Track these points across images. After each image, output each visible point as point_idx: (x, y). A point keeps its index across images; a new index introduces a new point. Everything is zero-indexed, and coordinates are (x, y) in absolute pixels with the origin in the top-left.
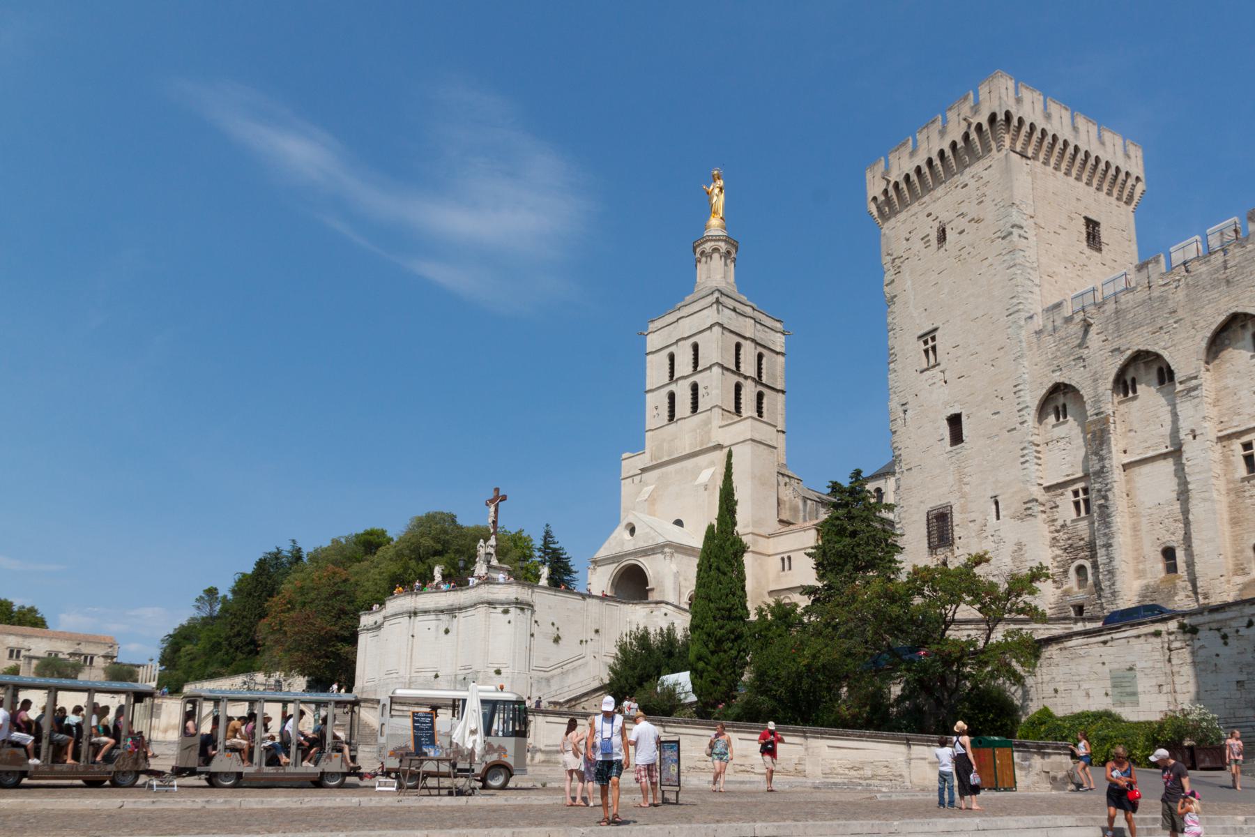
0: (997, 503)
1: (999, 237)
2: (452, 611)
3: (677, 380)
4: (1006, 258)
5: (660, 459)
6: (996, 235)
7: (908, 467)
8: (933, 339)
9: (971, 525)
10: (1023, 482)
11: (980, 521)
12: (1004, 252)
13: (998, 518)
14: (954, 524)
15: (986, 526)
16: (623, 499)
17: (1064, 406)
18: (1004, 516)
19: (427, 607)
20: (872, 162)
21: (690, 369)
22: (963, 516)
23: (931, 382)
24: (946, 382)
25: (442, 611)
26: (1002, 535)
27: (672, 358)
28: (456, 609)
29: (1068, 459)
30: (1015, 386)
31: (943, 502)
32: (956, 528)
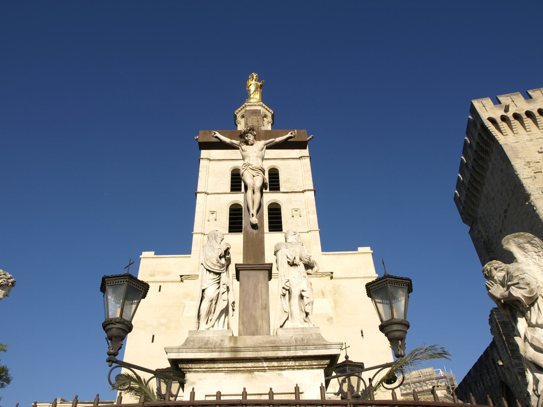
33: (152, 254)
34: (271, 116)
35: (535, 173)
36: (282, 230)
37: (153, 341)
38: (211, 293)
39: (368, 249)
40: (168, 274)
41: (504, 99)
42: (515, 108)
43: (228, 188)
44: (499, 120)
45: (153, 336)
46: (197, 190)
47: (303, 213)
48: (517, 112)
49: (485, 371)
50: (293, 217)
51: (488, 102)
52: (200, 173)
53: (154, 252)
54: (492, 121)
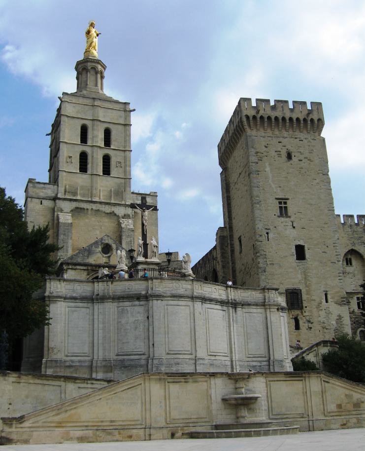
0: (326, 295)
2: (235, 305)
4: (326, 184)
6: (321, 172)
8: (285, 203)
10: (340, 288)
12: (325, 181)
13: (327, 302)
14: (303, 299)
15: (321, 304)
17: (350, 259)
18: (331, 302)
22: (308, 296)
23: (285, 224)
24: (294, 227)
26: (331, 310)
27: (84, 131)
29: (354, 283)
31: (296, 287)
38: (141, 251)
42: (263, 112)
44: (251, 118)
47: (123, 165)
48: (264, 115)
49: (207, 262)
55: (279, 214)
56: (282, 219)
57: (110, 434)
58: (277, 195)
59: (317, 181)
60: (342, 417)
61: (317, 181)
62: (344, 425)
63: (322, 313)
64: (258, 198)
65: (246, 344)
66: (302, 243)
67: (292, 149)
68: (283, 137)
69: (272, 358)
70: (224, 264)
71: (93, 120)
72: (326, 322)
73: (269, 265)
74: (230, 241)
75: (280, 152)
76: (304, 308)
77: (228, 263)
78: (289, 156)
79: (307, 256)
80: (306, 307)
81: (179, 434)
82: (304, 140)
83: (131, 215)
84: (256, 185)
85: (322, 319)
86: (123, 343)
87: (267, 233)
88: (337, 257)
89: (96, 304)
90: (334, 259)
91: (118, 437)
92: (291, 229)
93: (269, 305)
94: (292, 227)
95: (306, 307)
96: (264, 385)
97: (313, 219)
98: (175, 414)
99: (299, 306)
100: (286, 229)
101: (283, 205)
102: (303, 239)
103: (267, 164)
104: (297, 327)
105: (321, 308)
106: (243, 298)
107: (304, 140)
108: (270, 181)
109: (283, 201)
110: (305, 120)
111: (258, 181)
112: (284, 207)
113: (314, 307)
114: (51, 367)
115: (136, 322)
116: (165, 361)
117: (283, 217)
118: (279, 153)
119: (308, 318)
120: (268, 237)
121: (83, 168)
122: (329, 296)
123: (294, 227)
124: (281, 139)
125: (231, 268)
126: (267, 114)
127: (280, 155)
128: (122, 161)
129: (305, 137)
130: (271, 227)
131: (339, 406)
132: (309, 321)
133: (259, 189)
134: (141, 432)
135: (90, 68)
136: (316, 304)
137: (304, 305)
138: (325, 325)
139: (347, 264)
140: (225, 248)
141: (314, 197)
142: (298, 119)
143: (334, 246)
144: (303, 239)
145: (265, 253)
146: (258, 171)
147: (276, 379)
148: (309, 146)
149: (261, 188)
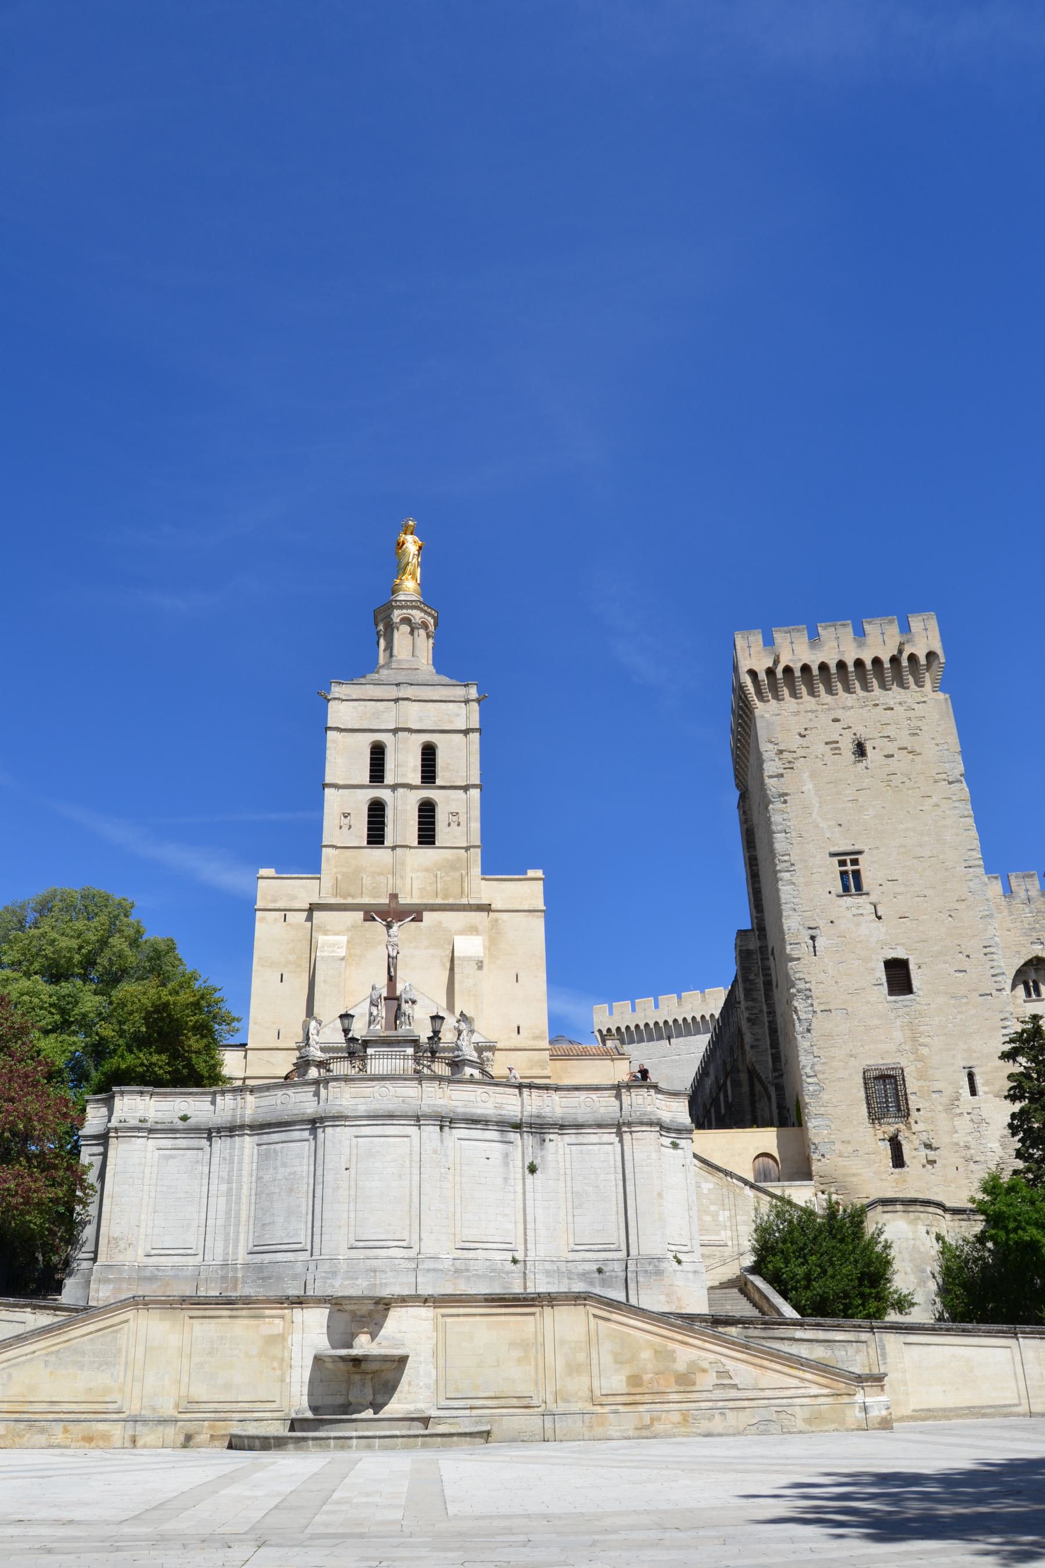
0: (971, 1076)
1: (945, 780)
3: (394, 787)
4: (957, 804)
5: (353, 897)
7: (823, 1007)
8: (855, 862)
9: (934, 1095)
11: (949, 1091)
12: (954, 798)
13: (973, 1092)
14: (908, 1091)
16: (257, 944)
18: (985, 1093)
19: (479, 1111)
20: (747, 626)
21: (416, 778)
22: (921, 1083)
23: (855, 911)
24: (879, 918)
25: (517, 1126)
26: (984, 1116)
27: (378, 753)
28: (553, 1125)
30: (985, 947)
32: (911, 1097)
33: (270, 872)
34: (432, 621)
35: (785, 769)
36: (433, 843)
37: (282, 981)
39: (539, 873)
40: (294, 898)
41: (780, 637)
43: (366, 779)
44: (762, 676)
45: (282, 975)
46: (324, 780)
47: (463, 819)
48: (791, 665)
50: (449, 825)
51: (757, 638)
52: (328, 752)
53: (273, 870)
54: (753, 673)
55: (840, 890)
56: (848, 901)
57: (43, 1431)
58: (834, 846)
59: (935, 800)
60: (642, 1408)
61: (935, 800)
62: (647, 1427)
63: (964, 1124)
64: (786, 858)
65: (570, 1218)
66: (900, 954)
67: (863, 732)
68: (844, 708)
69: (633, 1252)
70: (753, 1017)
71: (395, 731)
72: (973, 1144)
73: (819, 1014)
74: (761, 959)
75: (837, 742)
76: (914, 1114)
77: (761, 1011)
78: (860, 750)
79: (916, 983)
80: (918, 1110)
81: (204, 1437)
82: (897, 708)
83: (480, 928)
84: (779, 828)
85: (961, 1138)
86: (264, 1224)
87: (813, 938)
88: (995, 978)
89: (217, 1141)
90: (989, 986)
91: (59, 1437)
92: (871, 922)
93: (629, 1124)
94: (874, 916)
95: (918, 1110)
96: (429, 1326)
97: (926, 892)
98: (201, 1391)
99: (899, 1110)
100: (858, 925)
101: (849, 868)
102: (903, 944)
103: (806, 775)
104: (898, 1161)
105: (958, 1111)
106: (566, 1110)
107: (897, 708)
108: (814, 815)
109: (848, 858)
110: (895, 660)
111: (785, 816)
112: (853, 872)
113: (940, 1108)
114: (108, 1281)
115: (292, 1177)
116: (343, 1266)
117: (850, 895)
118: (835, 745)
119: (924, 1137)
120: (814, 947)
121: (376, 835)
122: (978, 1080)
123: (879, 918)
124: (839, 714)
125: (767, 1024)
126: (800, 660)
127: (836, 751)
128: (462, 811)
129: (898, 700)
130: (821, 923)
131: (635, 1380)
132: (928, 1146)
133: (788, 835)
134: (117, 1431)
135: (398, 621)
136: (945, 1100)
137: (912, 1106)
138: (973, 1151)
139: (1029, 994)
140: (752, 977)
141: (926, 838)
142: (877, 662)
143: (985, 954)
144: (903, 944)
145: (807, 986)
146: (786, 794)
147: (462, 1311)
148: (909, 719)
149: (794, 834)
